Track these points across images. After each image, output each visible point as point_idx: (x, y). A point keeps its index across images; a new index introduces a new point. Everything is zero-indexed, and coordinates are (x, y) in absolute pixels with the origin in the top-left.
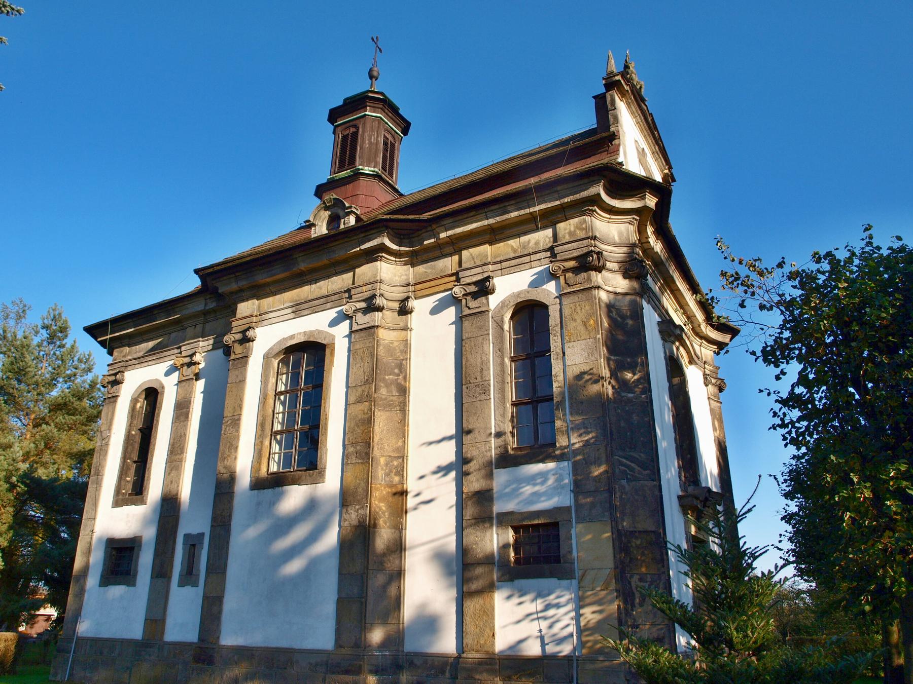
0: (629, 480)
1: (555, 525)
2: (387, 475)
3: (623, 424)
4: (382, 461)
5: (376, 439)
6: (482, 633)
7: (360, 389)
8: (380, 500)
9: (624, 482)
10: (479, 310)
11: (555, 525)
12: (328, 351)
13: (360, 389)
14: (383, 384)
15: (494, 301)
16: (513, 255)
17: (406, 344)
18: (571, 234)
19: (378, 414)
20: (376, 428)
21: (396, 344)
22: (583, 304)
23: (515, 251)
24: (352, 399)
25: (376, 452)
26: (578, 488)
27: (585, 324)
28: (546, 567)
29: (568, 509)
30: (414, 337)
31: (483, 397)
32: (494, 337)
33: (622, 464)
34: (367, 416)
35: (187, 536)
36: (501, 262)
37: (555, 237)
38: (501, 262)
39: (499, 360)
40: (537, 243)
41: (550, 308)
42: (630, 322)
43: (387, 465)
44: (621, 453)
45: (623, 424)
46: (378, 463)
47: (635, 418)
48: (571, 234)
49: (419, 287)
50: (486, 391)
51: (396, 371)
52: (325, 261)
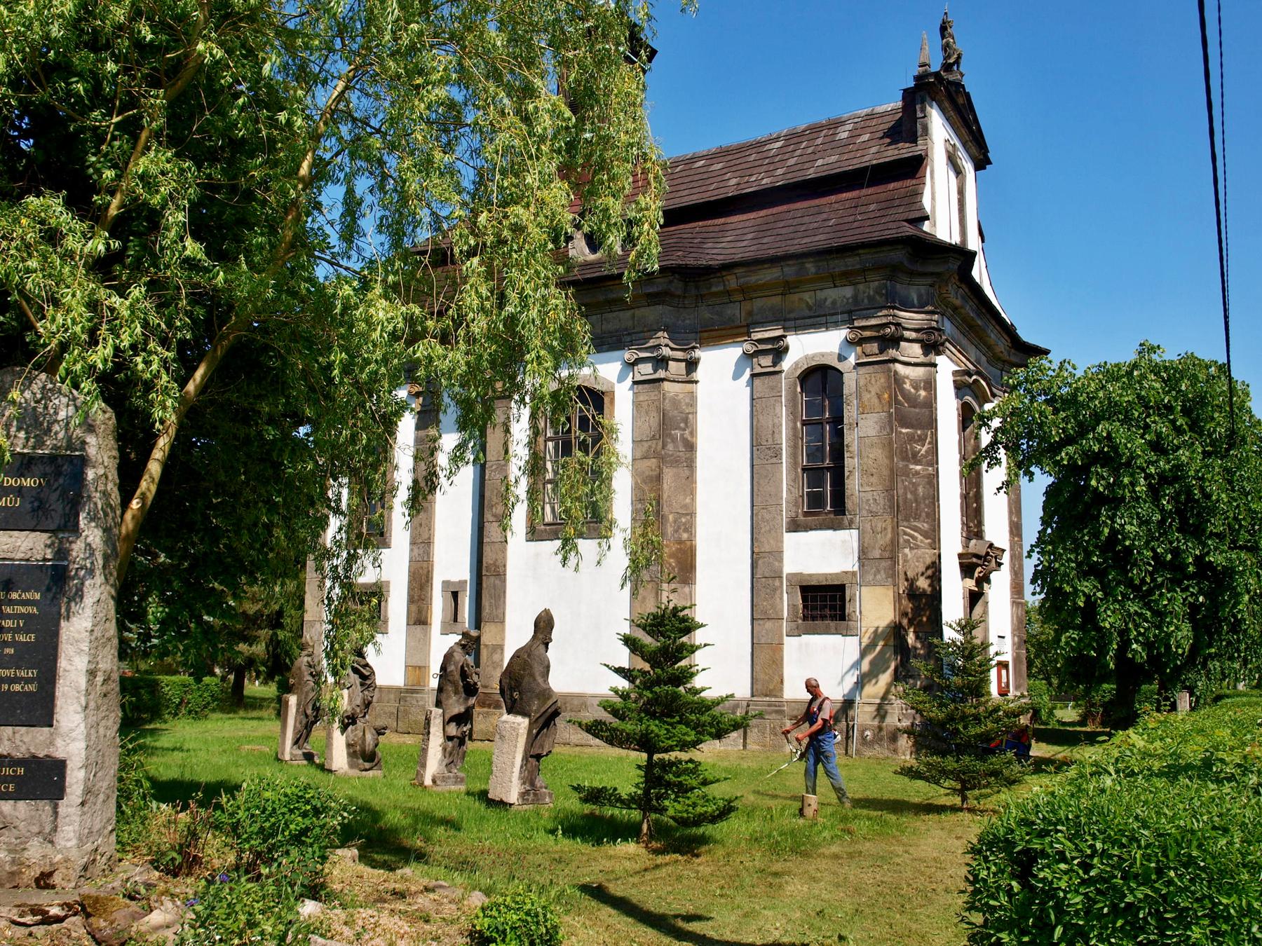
0: (911, 548)
1: (841, 588)
2: (676, 531)
3: (909, 496)
4: (671, 517)
5: (665, 496)
6: (771, 679)
7: (646, 445)
8: (670, 556)
9: (907, 551)
10: (772, 369)
11: (841, 588)
12: (606, 400)
13: (646, 445)
14: (670, 442)
15: (787, 364)
16: (807, 313)
17: (693, 397)
18: (870, 298)
19: (666, 470)
20: (665, 486)
21: (681, 396)
22: (878, 376)
23: (810, 308)
24: (638, 455)
25: (666, 510)
26: (863, 555)
27: (879, 397)
28: (832, 624)
29: (854, 573)
30: (700, 389)
31: (774, 460)
32: (787, 400)
33: (905, 533)
34: (655, 473)
35: (446, 584)
36: (795, 319)
37: (855, 297)
38: (795, 319)
39: (791, 425)
40: (834, 303)
41: (846, 377)
42: (923, 393)
43: (675, 522)
44: (905, 524)
45: (909, 496)
46: (667, 520)
47: (920, 490)
48: (869, 297)
49: (705, 335)
50: (778, 455)
51: (682, 425)
52: (601, 298)
